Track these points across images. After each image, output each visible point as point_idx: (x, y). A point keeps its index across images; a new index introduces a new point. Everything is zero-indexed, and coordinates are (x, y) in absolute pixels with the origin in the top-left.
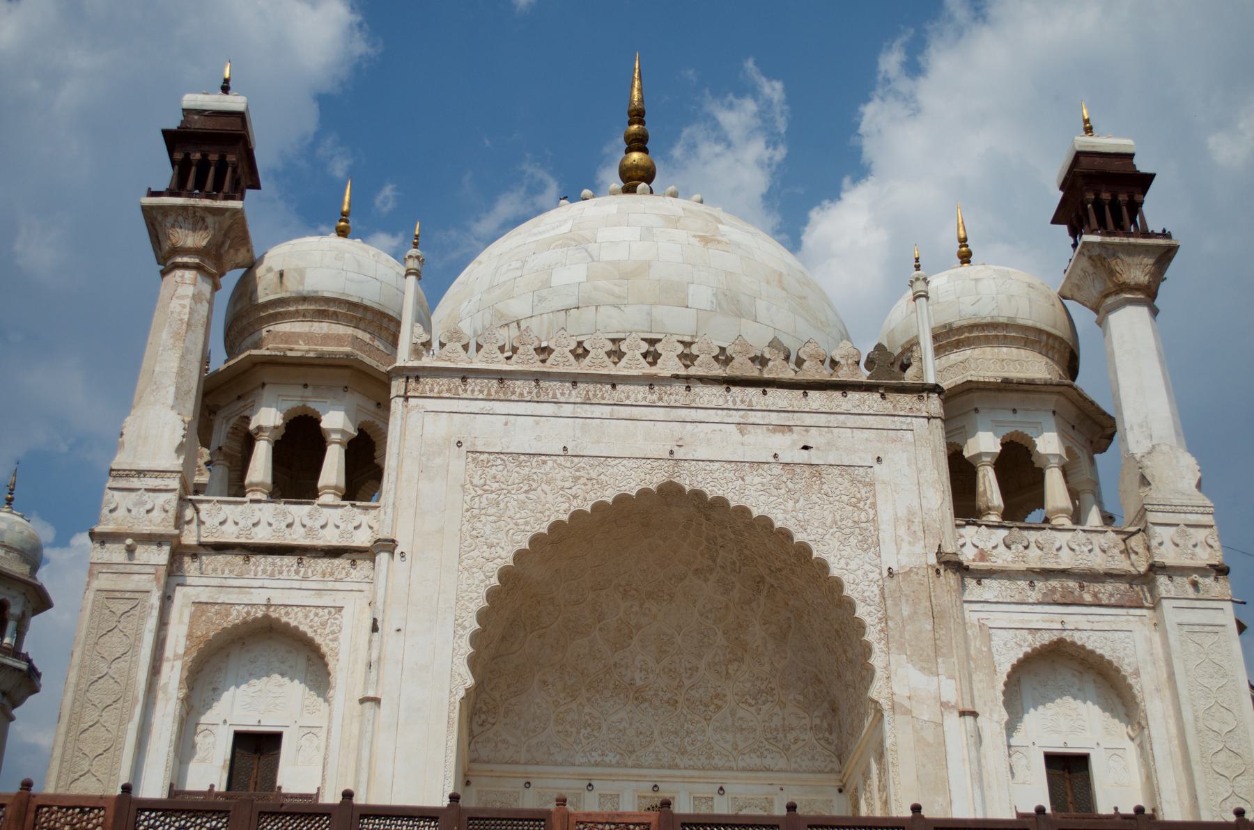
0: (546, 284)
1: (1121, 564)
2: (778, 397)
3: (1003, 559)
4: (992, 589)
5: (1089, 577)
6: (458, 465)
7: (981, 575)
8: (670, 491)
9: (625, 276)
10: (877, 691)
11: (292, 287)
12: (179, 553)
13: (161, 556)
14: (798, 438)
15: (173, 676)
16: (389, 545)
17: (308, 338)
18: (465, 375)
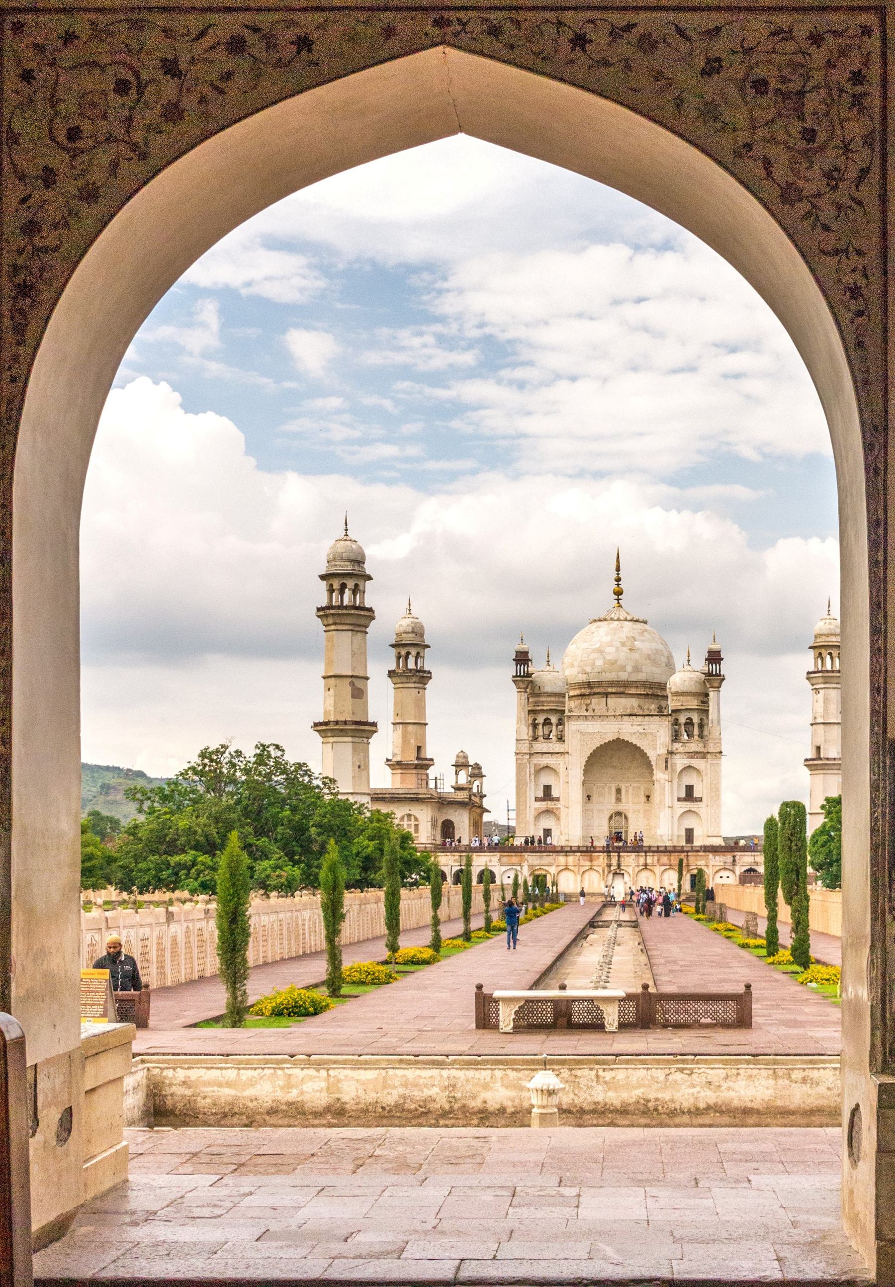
0: (594, 664)
1: (703, 750)
2: (639, 718)
3: (681, 750)
4: (678, 756)
5: (697, 753)
6: (579, 736)
7: (675, 754)
8: (618, 739)
9: (612, 664)
10: (654, 778)
11: (542, 690)
12: (530, 754)
13: (528, 757)
14: (642, 727)
15: (533, 777)
16: (567, 753)
17: (547, 702)
18: (579, 717)
